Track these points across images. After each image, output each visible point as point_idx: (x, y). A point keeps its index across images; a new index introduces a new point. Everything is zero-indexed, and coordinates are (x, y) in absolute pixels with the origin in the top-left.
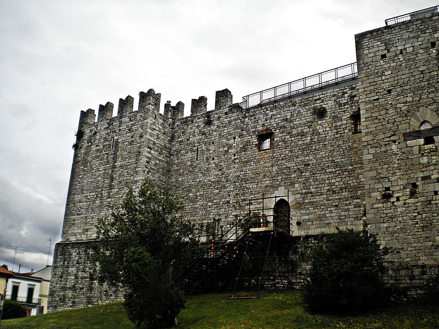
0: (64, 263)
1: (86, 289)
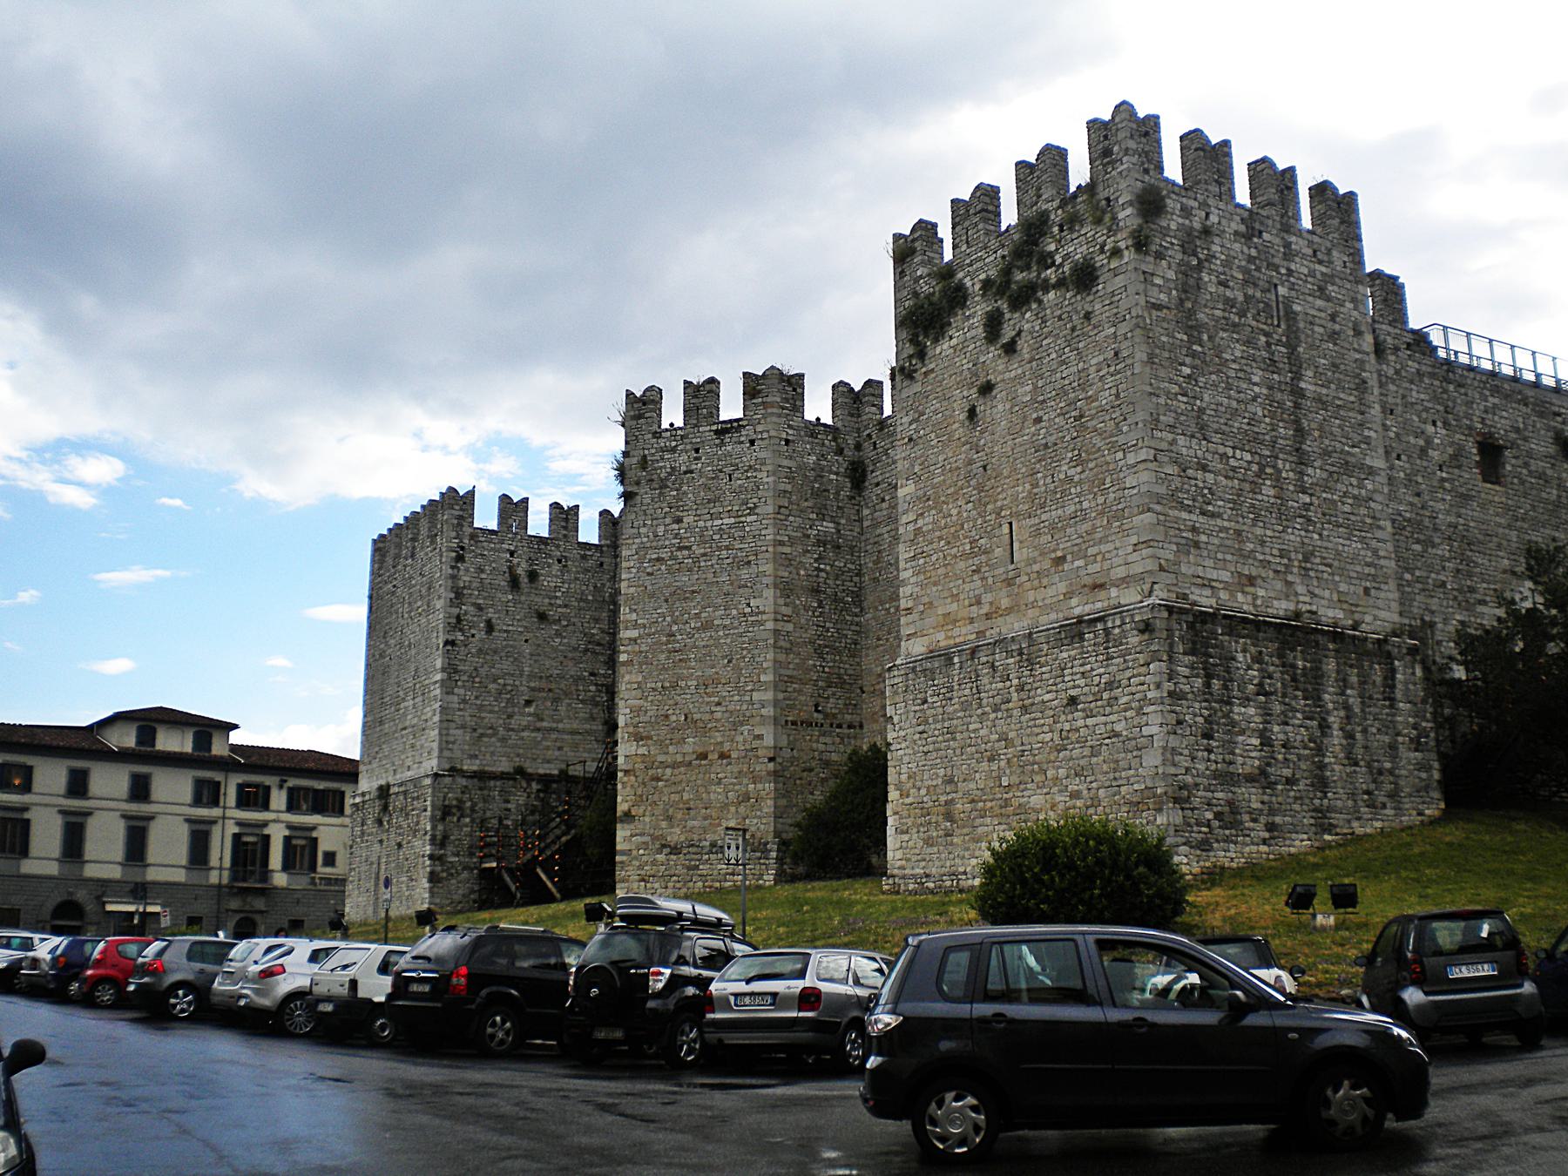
0: (1208, 685)
1: (1308, 782)
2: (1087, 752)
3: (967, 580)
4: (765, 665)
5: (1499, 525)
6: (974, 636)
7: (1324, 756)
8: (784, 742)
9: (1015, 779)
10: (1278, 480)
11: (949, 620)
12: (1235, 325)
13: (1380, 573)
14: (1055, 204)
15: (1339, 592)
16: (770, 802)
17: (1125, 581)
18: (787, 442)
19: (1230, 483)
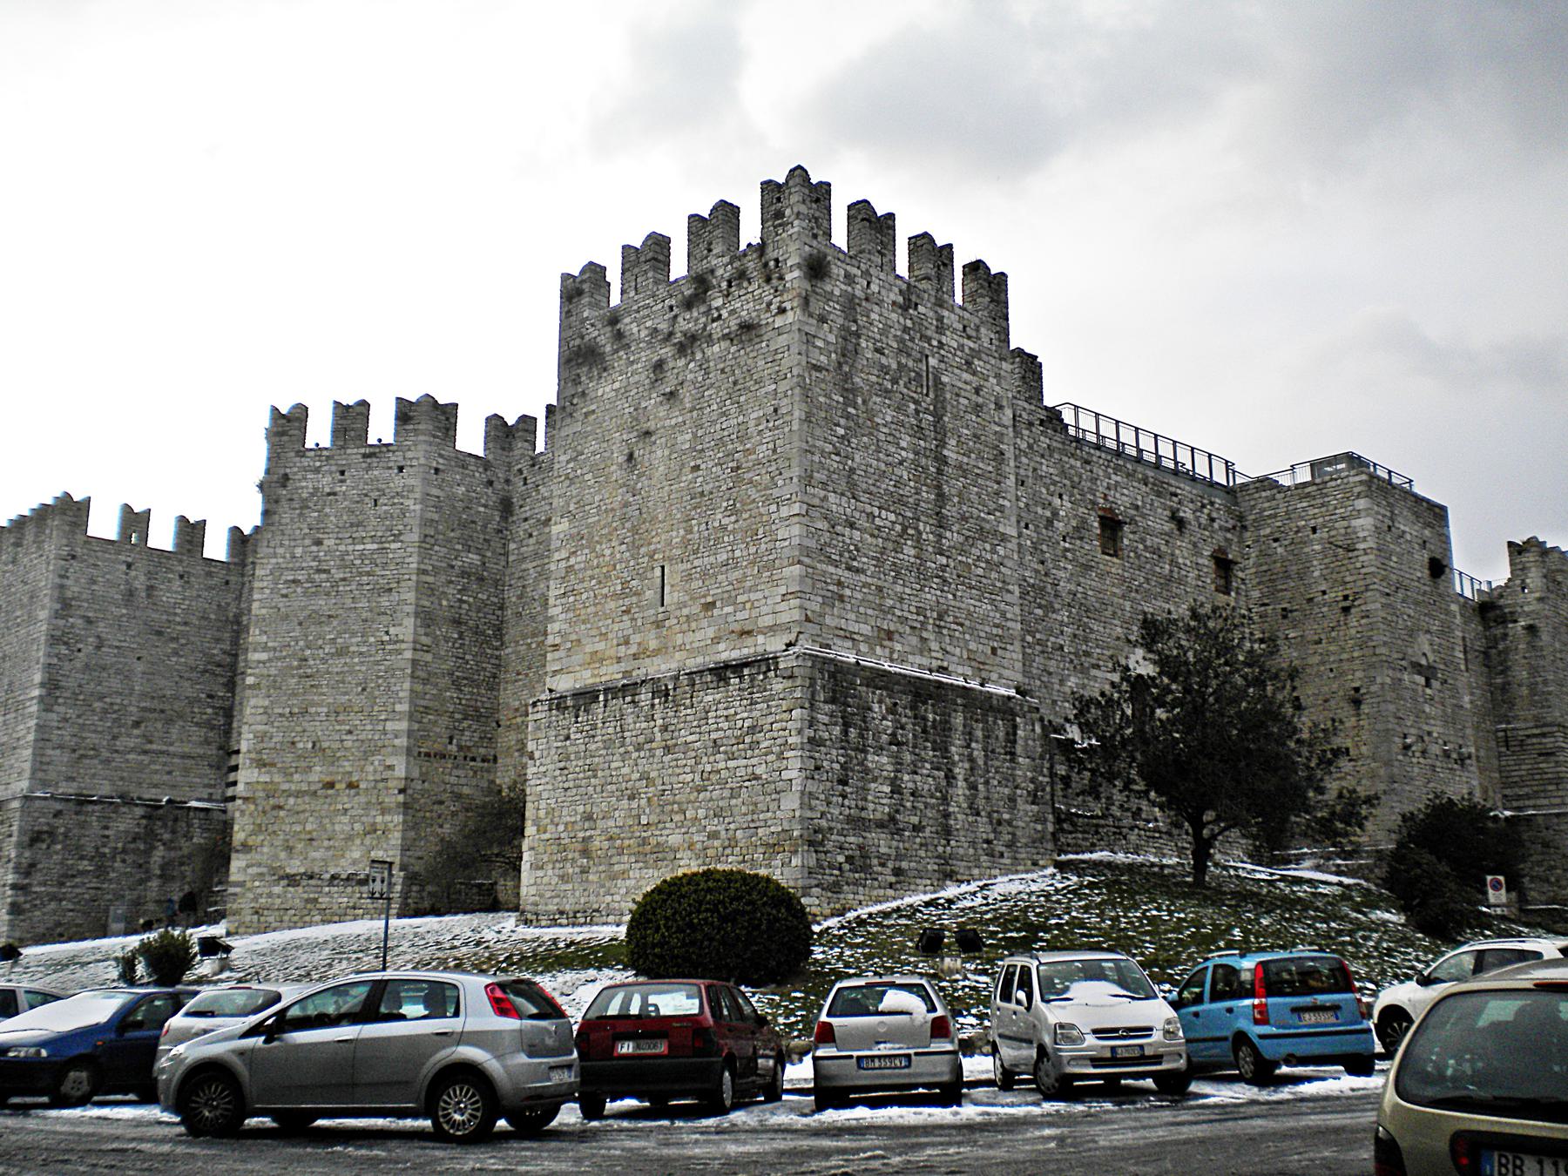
0: (845, 733)
1: (934, 829)
2: (726, 793)
3: (617, 620)
4: (401, 694)
5: (1114, 594)
6: (620, 675)
7: (948, 805)
8: (416, 774)
9: (654, 819)
10: (918, 542)
11: (597, 659)
12: (887, 391)
13: (1006, 634)
14: (726, 259)
15: (969, 650)
16: (398, 835)
17: (773, 629)
18: (437, 471)
19: (874, 541)
